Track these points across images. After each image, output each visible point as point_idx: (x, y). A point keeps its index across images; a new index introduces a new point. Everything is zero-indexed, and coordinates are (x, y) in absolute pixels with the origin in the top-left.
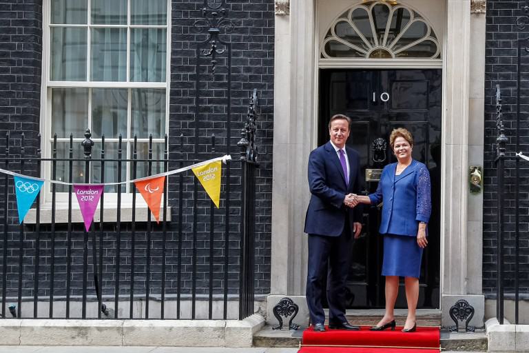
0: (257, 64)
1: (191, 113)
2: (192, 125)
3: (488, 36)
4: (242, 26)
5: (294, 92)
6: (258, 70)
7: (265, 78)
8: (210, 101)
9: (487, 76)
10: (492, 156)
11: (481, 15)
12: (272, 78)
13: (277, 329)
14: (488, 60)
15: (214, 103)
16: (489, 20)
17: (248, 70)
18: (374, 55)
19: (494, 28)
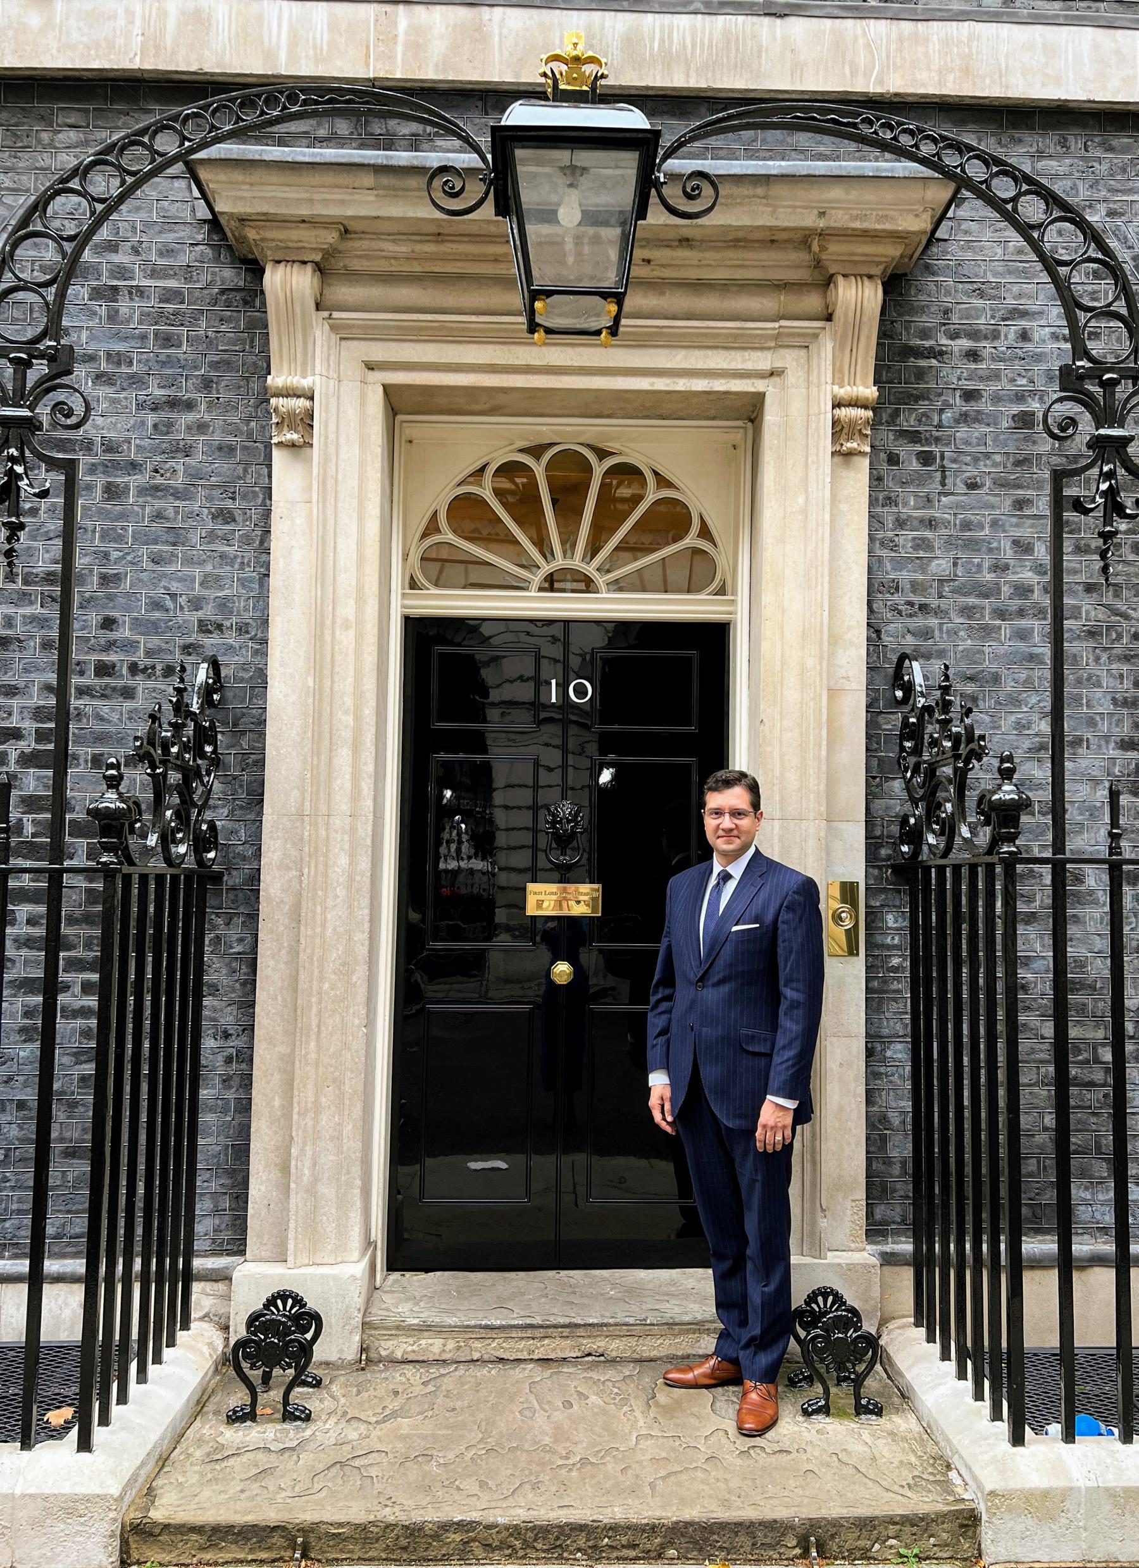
0: (222, 588)
1: (29, 725)
2: (27, 760)
3: (874, 520)
4: (179, 481)
5: (321, 662)
6: (224, 605)
7: (242, 629)
8: (82, 692)
9: (875, 630)
10: (884, 852)
11: (857, 460)
12: (265, 622)
13: (243, 1419)
14: (874, 588)
15: (93, 696)
16: (876, 479)
17: (196, 604)
18: (551, 583)
19: (890, 501)
